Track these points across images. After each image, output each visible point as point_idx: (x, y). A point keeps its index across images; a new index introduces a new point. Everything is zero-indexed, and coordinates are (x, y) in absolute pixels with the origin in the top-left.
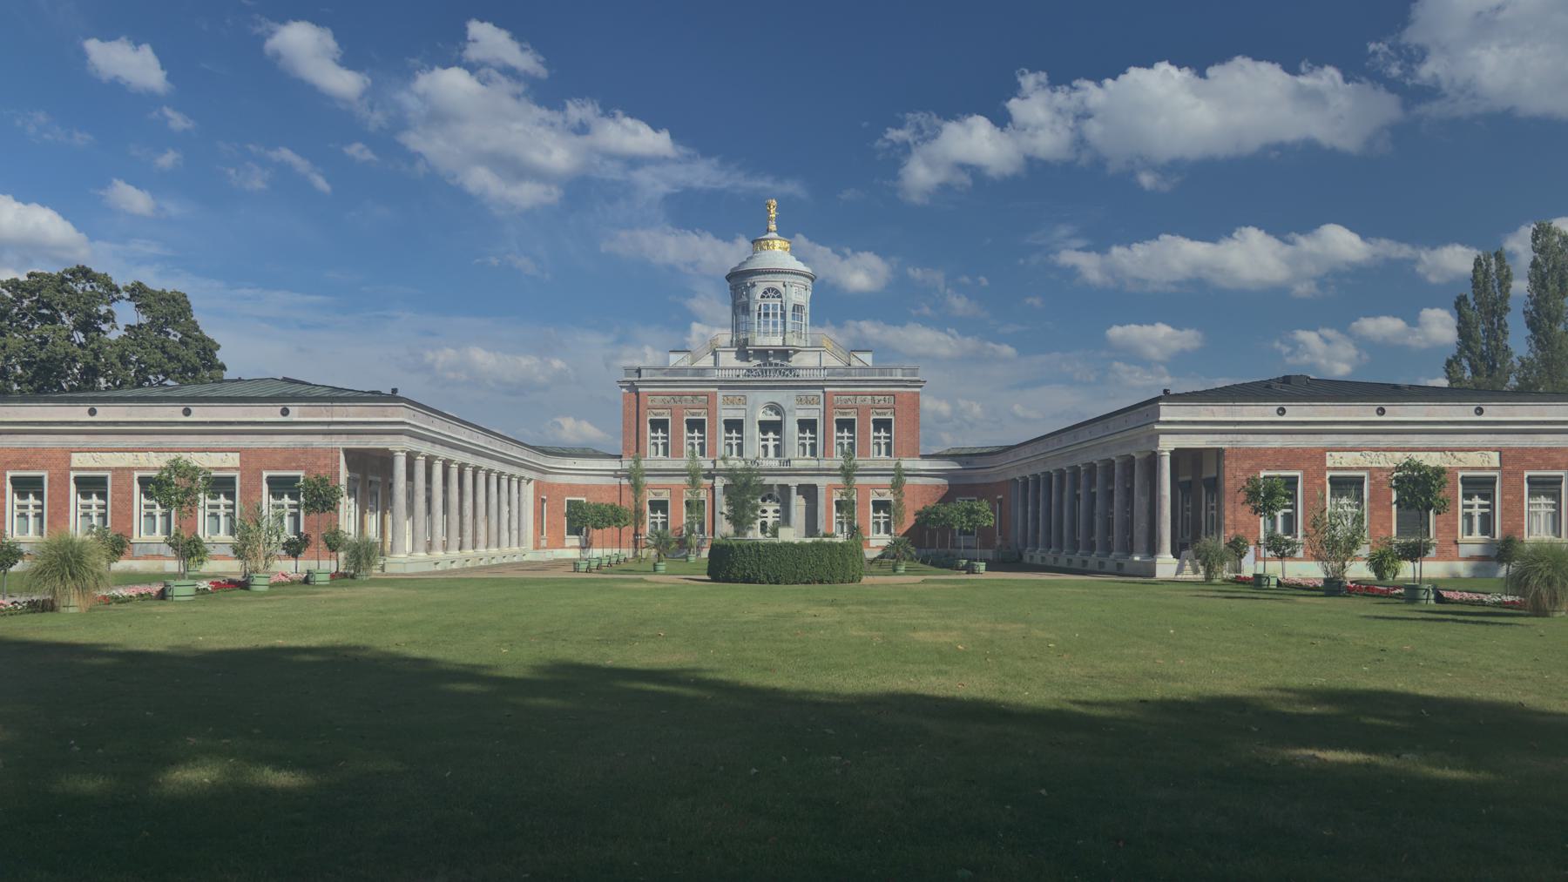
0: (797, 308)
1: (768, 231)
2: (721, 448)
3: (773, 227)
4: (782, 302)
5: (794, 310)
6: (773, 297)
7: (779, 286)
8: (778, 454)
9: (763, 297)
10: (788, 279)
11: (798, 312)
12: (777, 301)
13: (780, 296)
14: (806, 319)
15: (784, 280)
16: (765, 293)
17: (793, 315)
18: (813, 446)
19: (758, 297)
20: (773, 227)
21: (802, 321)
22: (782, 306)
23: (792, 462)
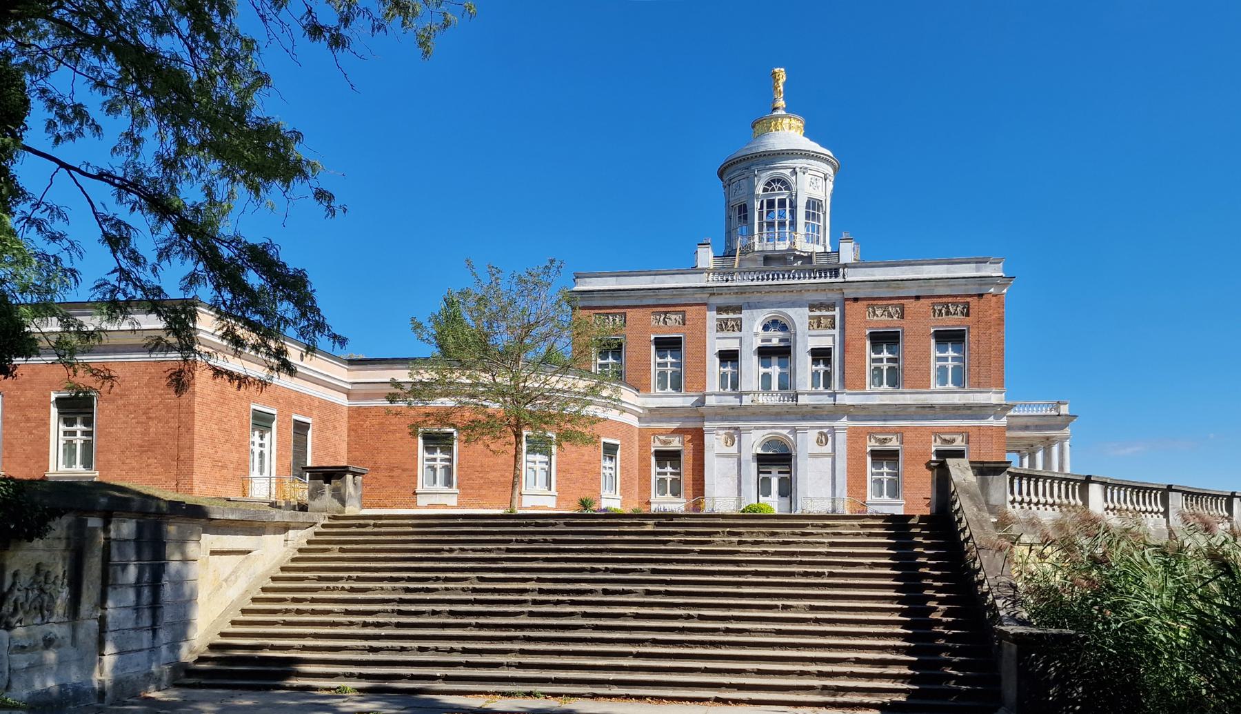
0: (813, 205)
1: (775, 109)
2: (713, 384)
3: (781, 103)
4: (791, 195)
5: (808, 206)
6: (780, 189)
7: (788, 172)
8: (782, 386)
9: (765, 190)
10: (799, 163)
11: (814, 209)
12: (784, 195)
13: (788, 188)
14: (826, 220)
15: (795, 165)
16: (768, 184)
17: (807, 217)
18: (828, 376)
19: (759, 190)
20: (781, 103)
21: (819, 222)
22: (791, 202)
23: (799, 396)
